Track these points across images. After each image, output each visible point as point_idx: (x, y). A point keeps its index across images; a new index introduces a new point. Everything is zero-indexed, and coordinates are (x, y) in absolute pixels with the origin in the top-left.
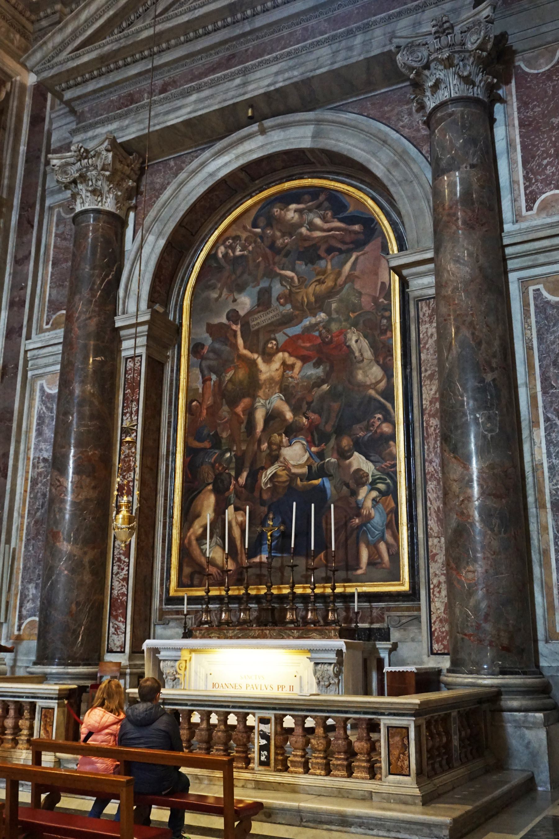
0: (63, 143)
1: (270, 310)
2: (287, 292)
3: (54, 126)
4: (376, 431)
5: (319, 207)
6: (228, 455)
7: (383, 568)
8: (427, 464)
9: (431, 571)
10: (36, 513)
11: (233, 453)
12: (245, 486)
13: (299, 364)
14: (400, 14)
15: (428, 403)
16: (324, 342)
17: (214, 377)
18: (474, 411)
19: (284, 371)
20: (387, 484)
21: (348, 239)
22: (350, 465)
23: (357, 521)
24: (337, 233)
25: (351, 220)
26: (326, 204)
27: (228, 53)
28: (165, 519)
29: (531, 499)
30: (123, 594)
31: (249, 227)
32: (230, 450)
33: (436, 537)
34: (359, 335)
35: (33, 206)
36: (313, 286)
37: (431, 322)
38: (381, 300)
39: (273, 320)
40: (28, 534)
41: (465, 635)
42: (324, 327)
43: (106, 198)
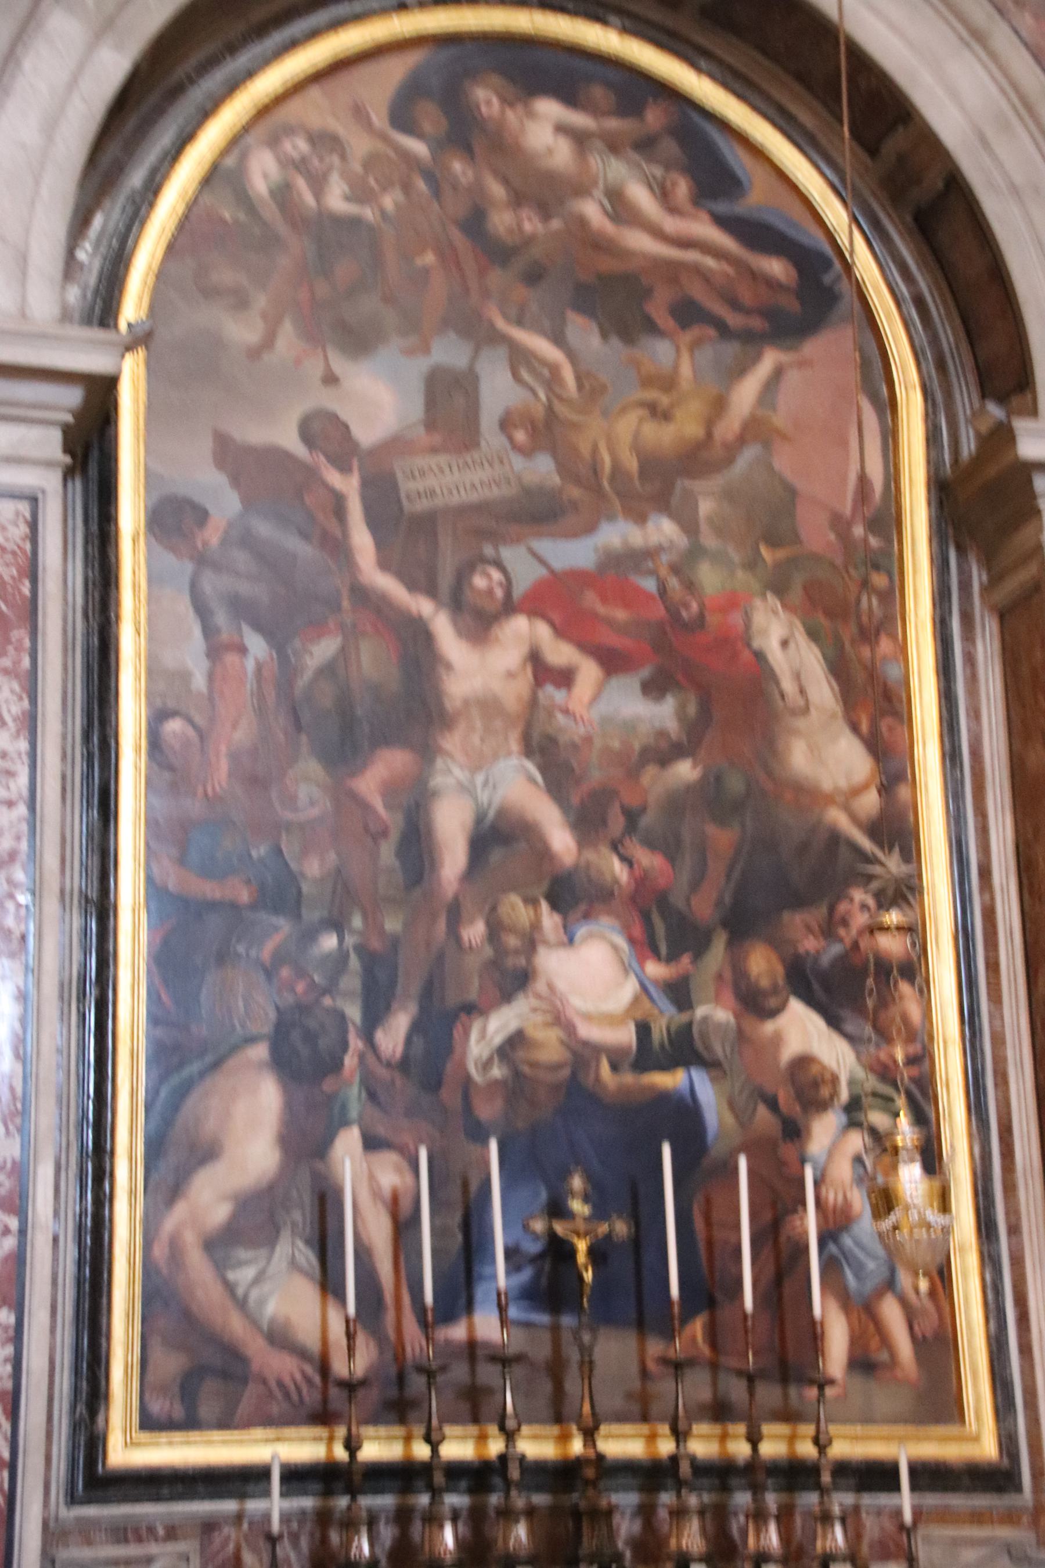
1: (476, 456)
2: (539, 412)
4: (856, 945)
5: (645, 145)
6: (329, 942)
11: (350, 940)
12: (404, 1065)
13: (589, 671)
16: (674, 614)
17: (257, 646)
21: (746, 295)
22: (777, 1041)
26: (670, 147)
31: (379, 119)
32: (338, 925)
34: (791, 625)
42: (675, 569)
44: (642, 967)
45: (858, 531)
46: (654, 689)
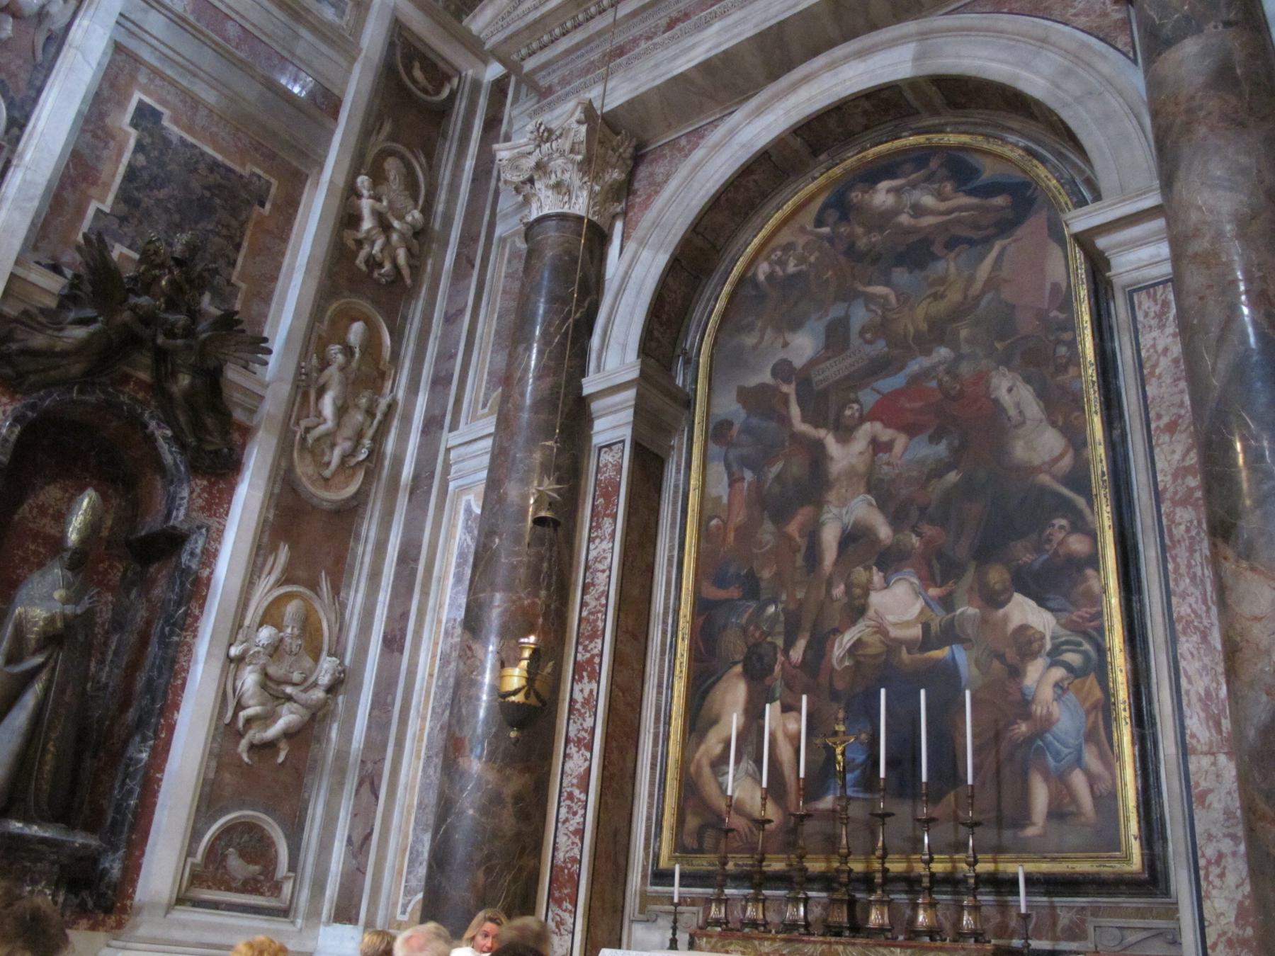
1: (848, 353)
2: (878, 319)
3: (516, 127)
4: (1056, 553)
5: (929, 179)
8: (1174, 600)
9: (1199, 829)
11: (780, 607)
12: (804, 664)
13: (901, 440)
15: (1169, 478)
17: (749, 475)
19: (875, 453)
20: (1085, 654)
22: (1006, 618)
23: (1023, 728)
28: (656, 727)
31: (809, 227)
32: (774, 601)
33: (1206, 754)
35: (475, 239)
36: (924, 304)
37: (1162, 327)
38: (1052, 315)
40: (428, 749)
42: (948, 372)
43: (577, 197)
44: (926, 591)
45: (1054, 314)
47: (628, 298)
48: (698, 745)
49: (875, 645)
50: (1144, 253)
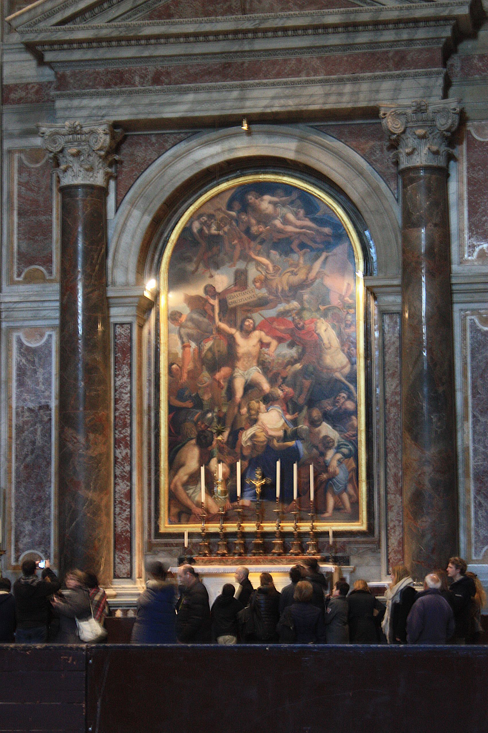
0: (18, 81)
4: (341, 407)
5: (292, 203)
7: (345, 513)
8: (388, 441)
9: (389, 517)
10: (25, 458)
11: (215, 414)
12: (227, 443)
13: (274, 343)
14: (384, 77)
16: (296, 326)
17: (193, 345)
18: (430, 413)
20: (350, 450)
22: (319, 432)
23: (325, 476)
24: (308, 231)
25: (321, 222)
26: (299, 202)
27: (224, 61)
29: (460, 471)
30: (127, 531)
31: (224, 208)
33: (392, 494)
39: (249, 300)
40: (17, 477)
41: (419, 562)
46: (291, 345)
47: (126, 239)
48: (174, 475)
49: (262, 437)
50: (391, 299)
